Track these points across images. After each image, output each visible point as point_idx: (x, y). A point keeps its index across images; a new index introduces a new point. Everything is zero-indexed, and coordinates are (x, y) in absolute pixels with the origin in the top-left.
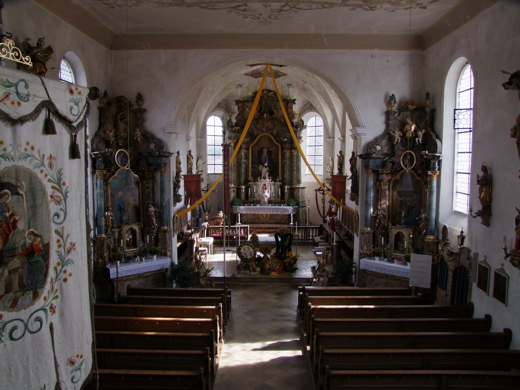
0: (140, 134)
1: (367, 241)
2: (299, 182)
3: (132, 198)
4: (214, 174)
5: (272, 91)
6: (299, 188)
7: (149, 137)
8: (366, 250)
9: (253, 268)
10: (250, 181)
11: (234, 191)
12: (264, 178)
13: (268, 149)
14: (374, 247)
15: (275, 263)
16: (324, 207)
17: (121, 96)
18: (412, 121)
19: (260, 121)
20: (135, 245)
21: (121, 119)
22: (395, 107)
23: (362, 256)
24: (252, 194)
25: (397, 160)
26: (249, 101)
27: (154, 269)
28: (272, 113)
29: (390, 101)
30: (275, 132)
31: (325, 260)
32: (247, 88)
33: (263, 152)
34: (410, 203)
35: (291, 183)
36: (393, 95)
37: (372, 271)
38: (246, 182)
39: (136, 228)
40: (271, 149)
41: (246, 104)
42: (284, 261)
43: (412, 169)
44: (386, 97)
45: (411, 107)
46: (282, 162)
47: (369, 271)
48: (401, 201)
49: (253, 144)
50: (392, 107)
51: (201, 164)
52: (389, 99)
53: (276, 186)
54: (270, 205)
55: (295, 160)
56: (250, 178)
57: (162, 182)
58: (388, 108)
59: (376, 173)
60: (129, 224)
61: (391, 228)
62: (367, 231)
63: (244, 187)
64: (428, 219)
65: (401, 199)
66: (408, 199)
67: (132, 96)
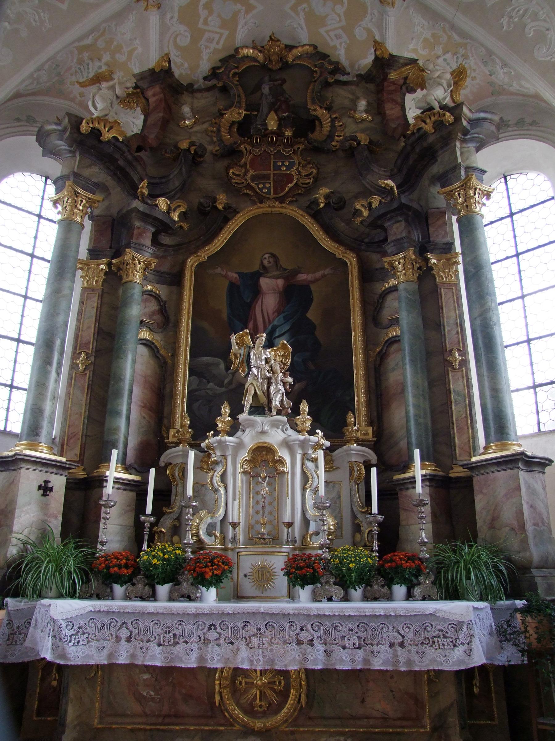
11: (46, 489)
12: (261, 408)
13: (289, 276)
28: (305, 125)
33: (257, 292)
40: (302, 277)
46: (367, 341)
49: (204, 255)
53: (342, 475)
54: (304, 594)
56: (181, 420)
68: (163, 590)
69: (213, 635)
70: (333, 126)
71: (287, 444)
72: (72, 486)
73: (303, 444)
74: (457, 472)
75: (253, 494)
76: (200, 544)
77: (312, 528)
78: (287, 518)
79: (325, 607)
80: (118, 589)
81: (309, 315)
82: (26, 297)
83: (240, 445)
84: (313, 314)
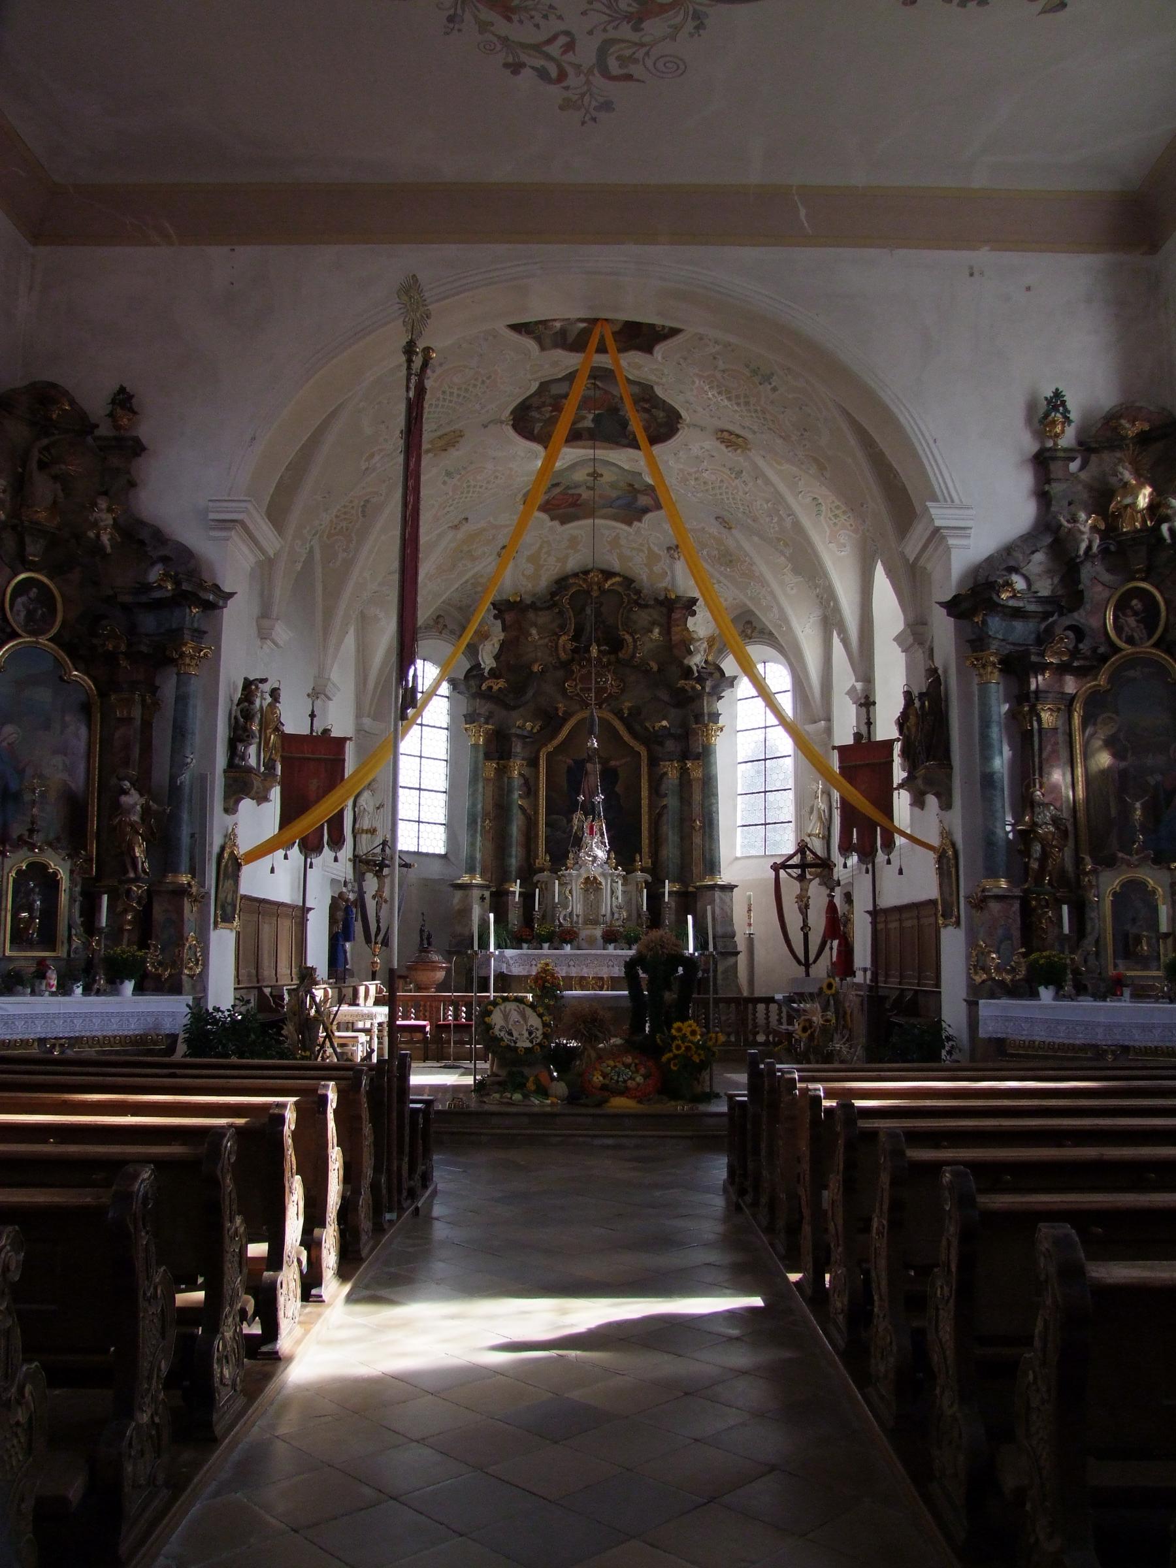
0: (111, 522)
1: (1000, 932)
2: (712, 866)
3: (58, 760)
4: (418, 853)
5: (614, 574)
6: (713, 887)
7: (143, 540)
8: (998, 969)
9: (537, 1082)
10: (542, 870)
11: (483, 898)
13: (604, 762)
15: (628, 1066)
16: (805, 927)
17: (54, 386)
18: (1138, 474)
19: (575, 668)
20: (48, 939)
21: (42, 466)
22: (1068, 438)
24: (548, 915)
25: (1094, 623)
26: (538, 604)
27: (113, 1029)
28: (615, 645)
29: (1047, 415)
30: (628, 704)
31: (830, 1014)
32: (533, 559)
34: (1159, 777)
35: (683, 875)
36: (1057, 394)
38: (528, 874)
39: (60, 867)
40: (613, 763)
41: (531, 615)
42: (664, 1059)
43: (1155, 645)
44: (1031, 407)
45: (1131, 430)
46: (651, 806)
50: (1057, 436)
51: (371, 809)
52: (1043, 406)
53: (632, 888)
54: (611, 946)
55: (697, 797)
56: (542, 858)
57: (182, 700)
58: (1042, 442)
59: (1016, 667)
60: (32, 847)
61: (1094, 871)
62: (996, 891)
63: (516, 888)
67: (95, 401)
68: (546, 945)
69: (572, 963)
70: (635, 647)
71: (603, 875)
72: (492, 894)
73: (612, 875)
74: (691, 889)
75: (586, 899)
76: (561, 925)
77: (616, 916)
78: (603, 912)
79: (619, 952)
80: (525, 945)
81: (617, 789)
82: (421, 757)
83: (579, 876)
84: (618, 789)
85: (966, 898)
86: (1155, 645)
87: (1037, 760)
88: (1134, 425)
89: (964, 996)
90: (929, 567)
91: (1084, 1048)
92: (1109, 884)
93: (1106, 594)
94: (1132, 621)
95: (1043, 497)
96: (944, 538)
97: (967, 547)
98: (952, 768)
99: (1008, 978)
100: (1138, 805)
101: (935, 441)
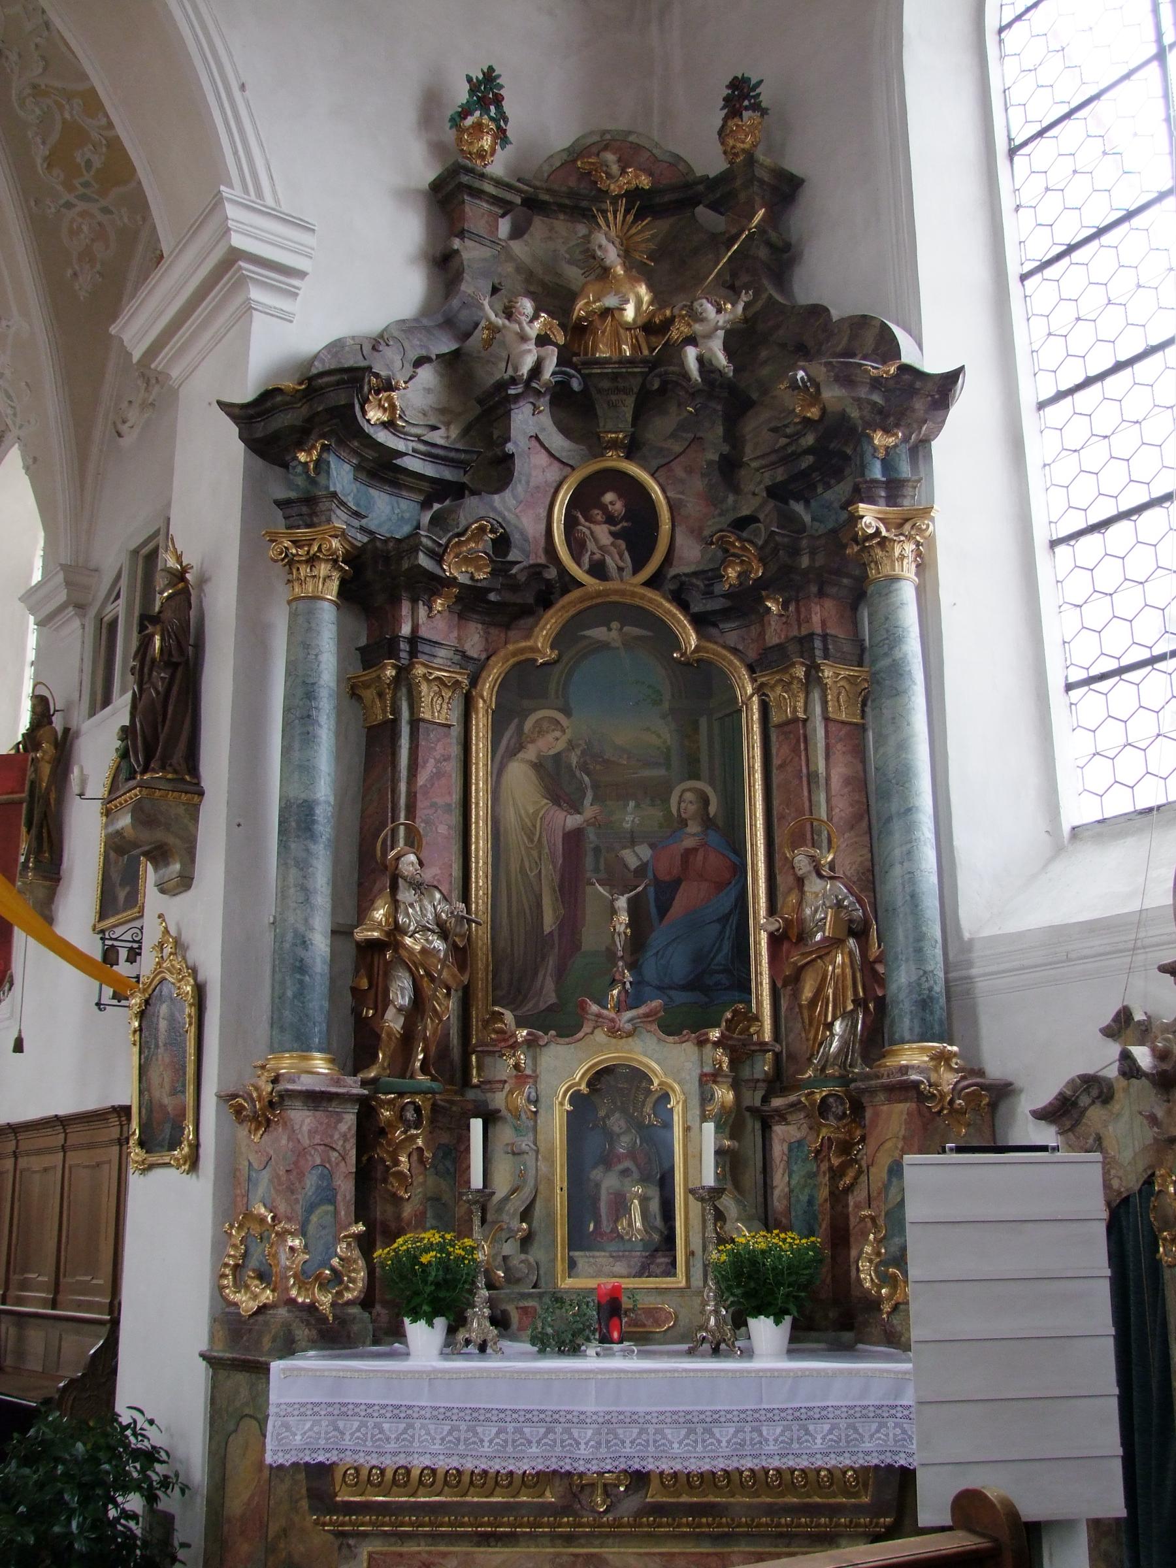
1: (311, 1181)
8: (304, 1278)
14: (366, 1244)
23: (239, 1359)
29: (465, 112)
34: (645, 852)
37: (402, 1478)
43: (651, 583)
47: (375, 1478)
48: (573, 839)
62: (306, 1083)
64: (871, 918)
65: (573, 821)
66: (629, 818)
85: (227, 1098)
86: (651, 583)
87: (403, 787)
88: (623, 172)
89: (202, 1343)
90: (174, 373)
91: (542, 1479)
92: (564, 1069)
93: (553, 473)
94: (603, 532)
95: (443, 265)
96: (241, 282)
97: (287, 318)
98: (201, 794)
99: (325, 1300)
100: (622, 902)
101: (243, 87)
